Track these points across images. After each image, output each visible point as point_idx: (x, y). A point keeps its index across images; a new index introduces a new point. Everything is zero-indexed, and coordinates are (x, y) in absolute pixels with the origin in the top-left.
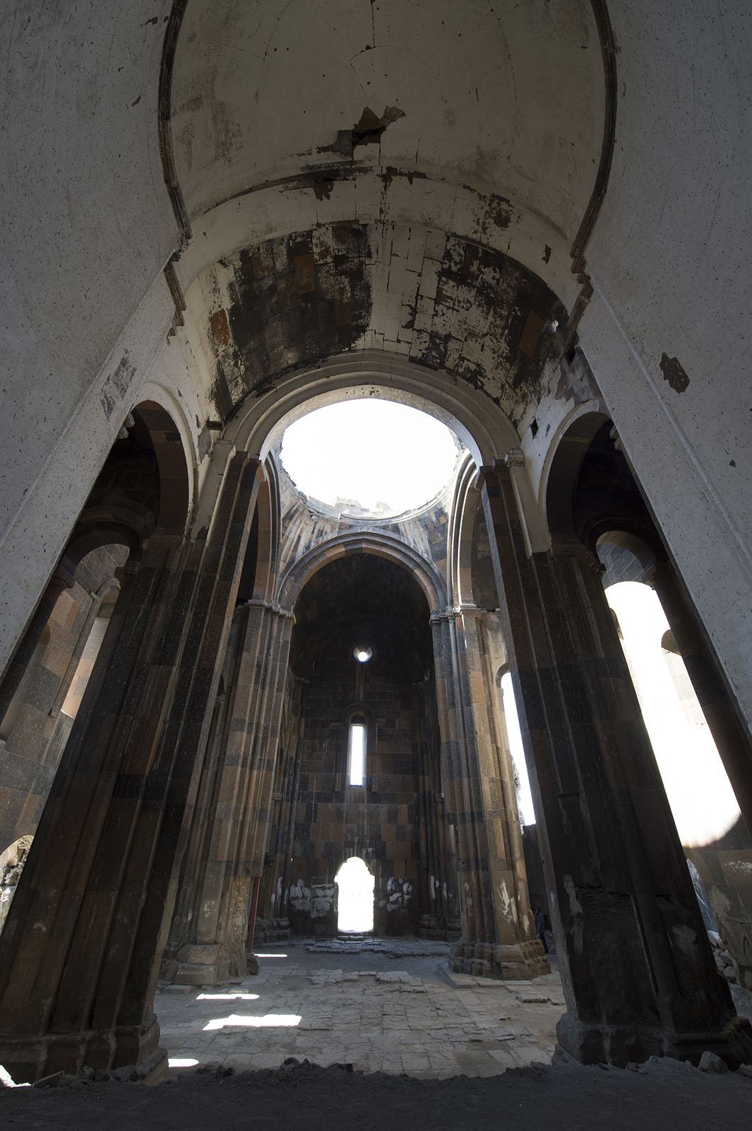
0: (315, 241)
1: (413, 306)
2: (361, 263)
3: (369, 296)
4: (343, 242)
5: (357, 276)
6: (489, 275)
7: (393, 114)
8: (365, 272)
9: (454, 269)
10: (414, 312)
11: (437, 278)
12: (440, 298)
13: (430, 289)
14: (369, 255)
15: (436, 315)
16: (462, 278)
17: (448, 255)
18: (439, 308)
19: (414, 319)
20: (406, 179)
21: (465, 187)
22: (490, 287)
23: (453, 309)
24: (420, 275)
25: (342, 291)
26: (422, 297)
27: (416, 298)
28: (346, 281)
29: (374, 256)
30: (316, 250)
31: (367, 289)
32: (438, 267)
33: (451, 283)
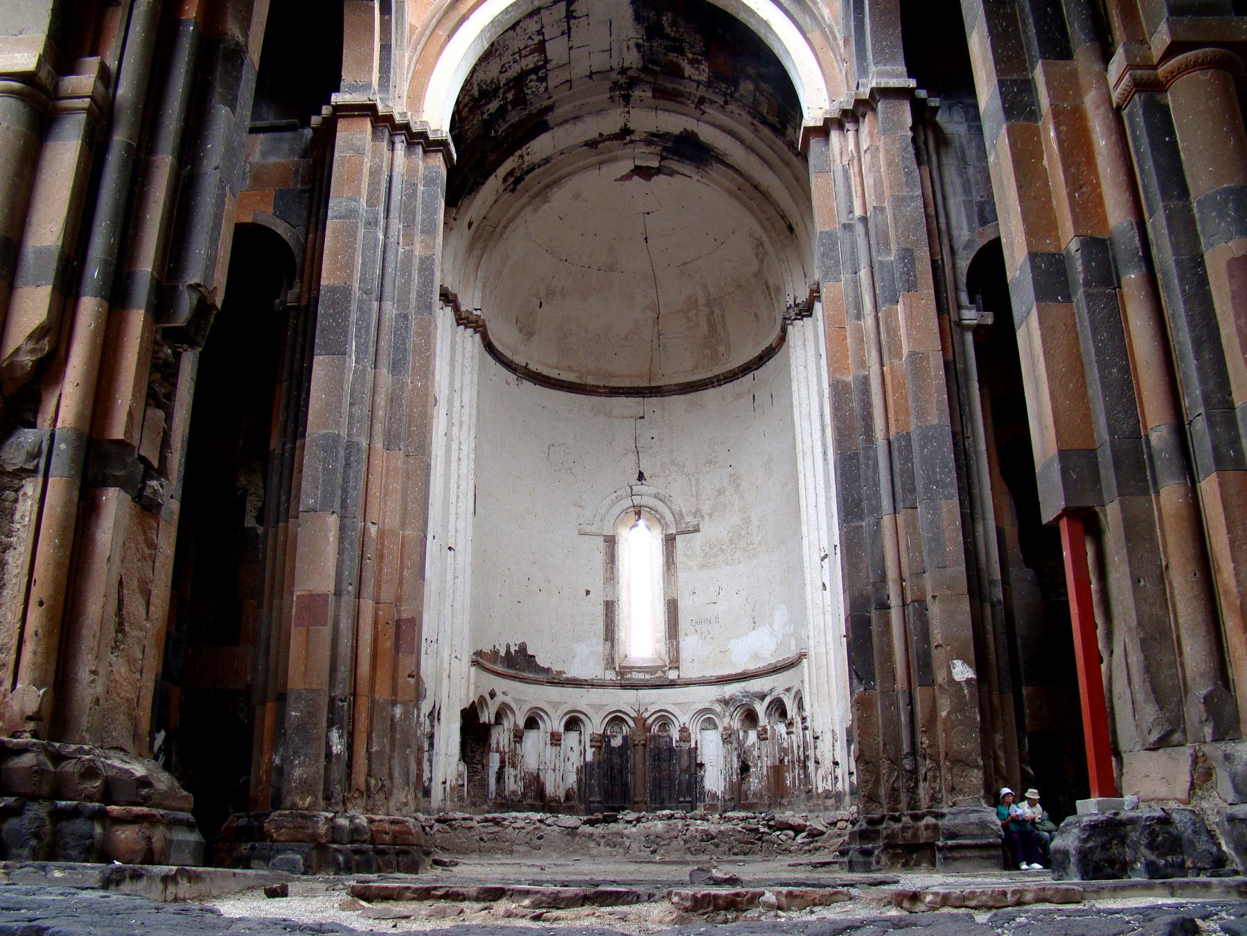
0: (706, 75)
1: (572, 21)
2: (648, 40)
3: (635, 11)
4: (671, 62)
5: (653, 31)
6: (493, 106)
7: (627, 177)
8: (642, 32)
9: (534, 77)
10: (570, 16)
11: (549, 57)
12: (541, 48)
13: (556, 50)
14: (638, 46)
15: (540, 32)
16: (519, 81)
17: (542, 80)
18: (537, 39)
19: (568, 10)
20: (605, 133)
21: (547, 160)
22: (488, 103)
23: (520, 51)
24: (570, 48)
25: (674, 24)
26: (563, 33)
27: (569, 28)
28: (668, 30)
29: (632, 43)
30: (704, 66)
31: (638, 18)
32: (549, 67)
33: (531, 66)
